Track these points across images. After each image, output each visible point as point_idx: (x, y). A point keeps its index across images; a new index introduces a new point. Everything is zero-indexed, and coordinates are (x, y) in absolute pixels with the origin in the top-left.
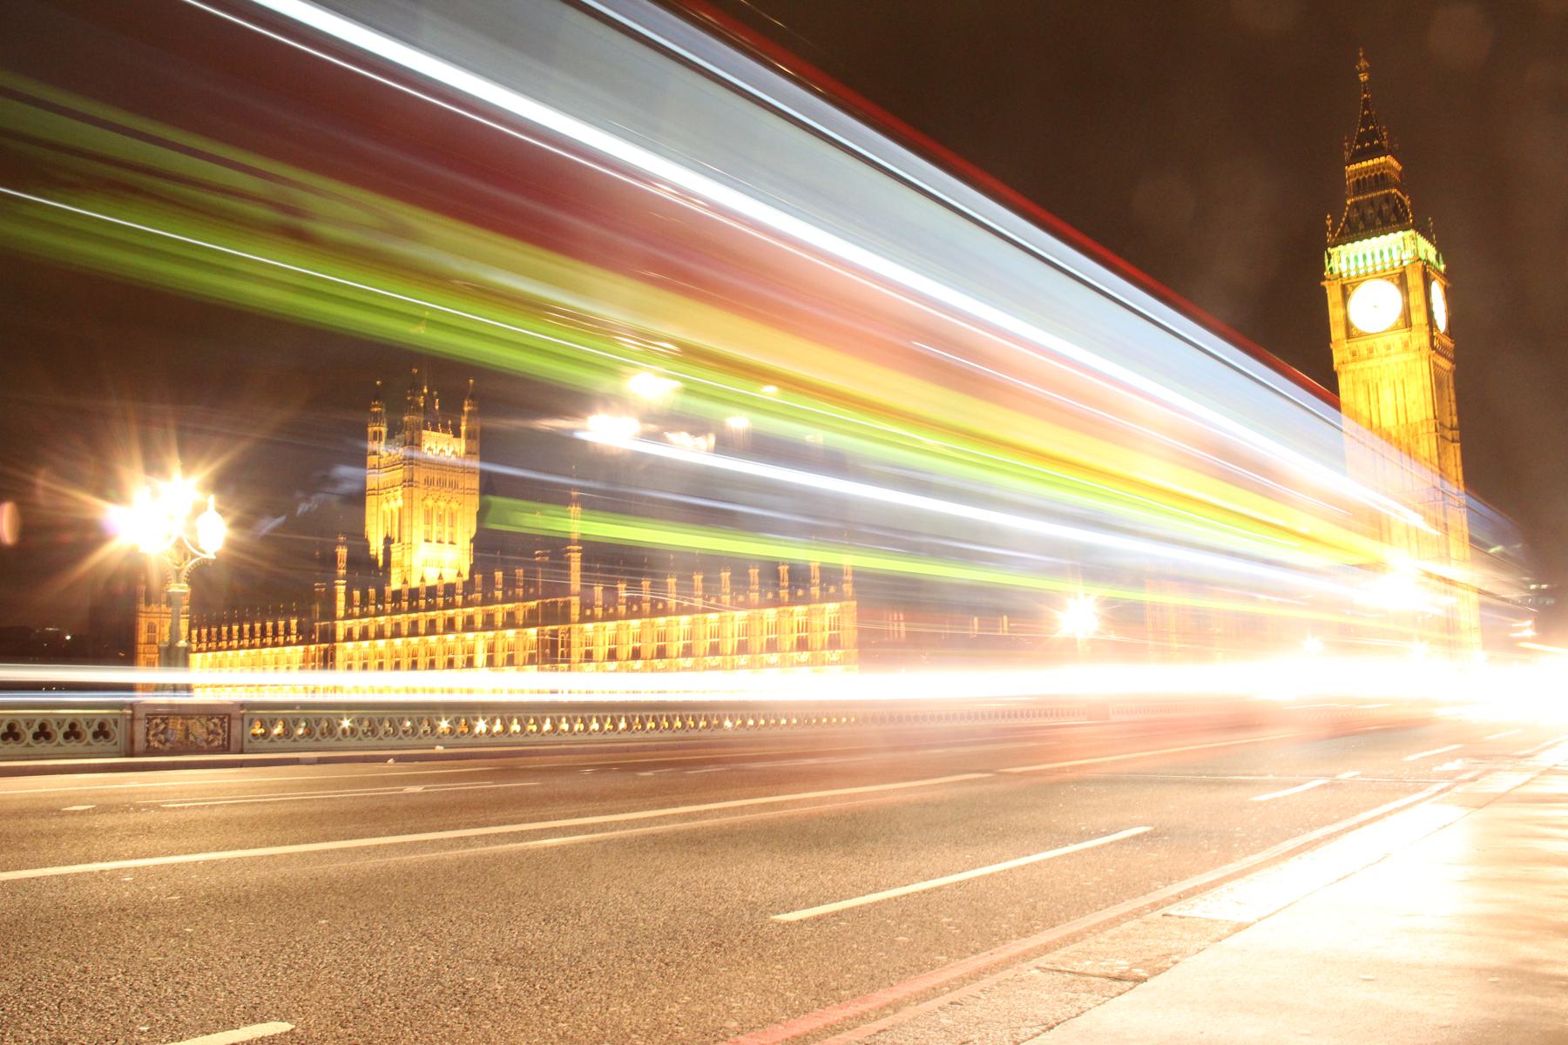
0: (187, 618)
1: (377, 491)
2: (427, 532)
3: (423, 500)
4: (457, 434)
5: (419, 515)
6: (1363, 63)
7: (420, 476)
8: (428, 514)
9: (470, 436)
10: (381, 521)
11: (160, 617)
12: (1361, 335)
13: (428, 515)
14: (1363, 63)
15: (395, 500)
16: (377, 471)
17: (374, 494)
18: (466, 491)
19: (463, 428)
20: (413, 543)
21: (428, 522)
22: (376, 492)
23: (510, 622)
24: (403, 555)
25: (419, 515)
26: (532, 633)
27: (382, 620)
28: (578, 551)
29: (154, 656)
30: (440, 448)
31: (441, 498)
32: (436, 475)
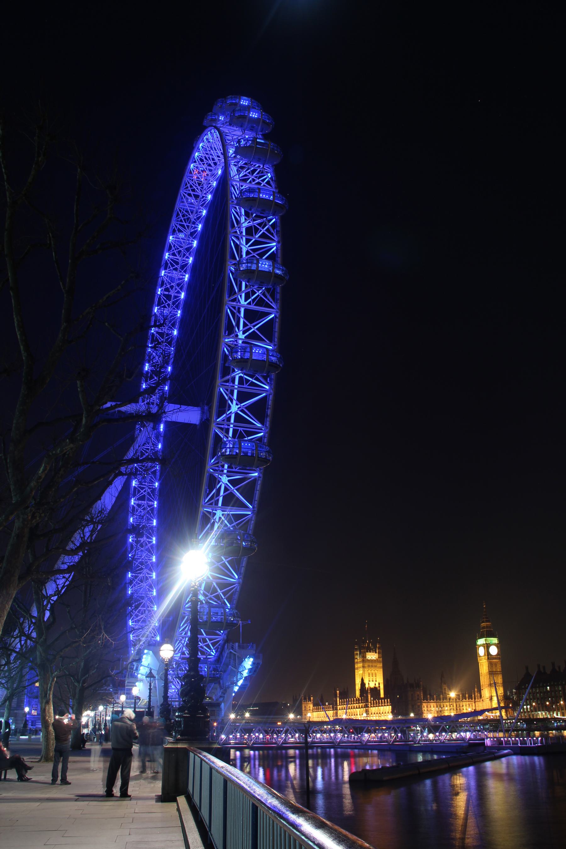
1: (358, 668)
4: (376, 653)
6: (484, 604)
7: (366, 665)
8: (369, 674)
9: (378, 654)
12: (481, 656)
14: (484, 604)
18: (379, 667)
19: (377, 651)
21: (369, 676)
23: (362, 707)
25: (367, 675)
26: (365, 709)
27: (344, 706)
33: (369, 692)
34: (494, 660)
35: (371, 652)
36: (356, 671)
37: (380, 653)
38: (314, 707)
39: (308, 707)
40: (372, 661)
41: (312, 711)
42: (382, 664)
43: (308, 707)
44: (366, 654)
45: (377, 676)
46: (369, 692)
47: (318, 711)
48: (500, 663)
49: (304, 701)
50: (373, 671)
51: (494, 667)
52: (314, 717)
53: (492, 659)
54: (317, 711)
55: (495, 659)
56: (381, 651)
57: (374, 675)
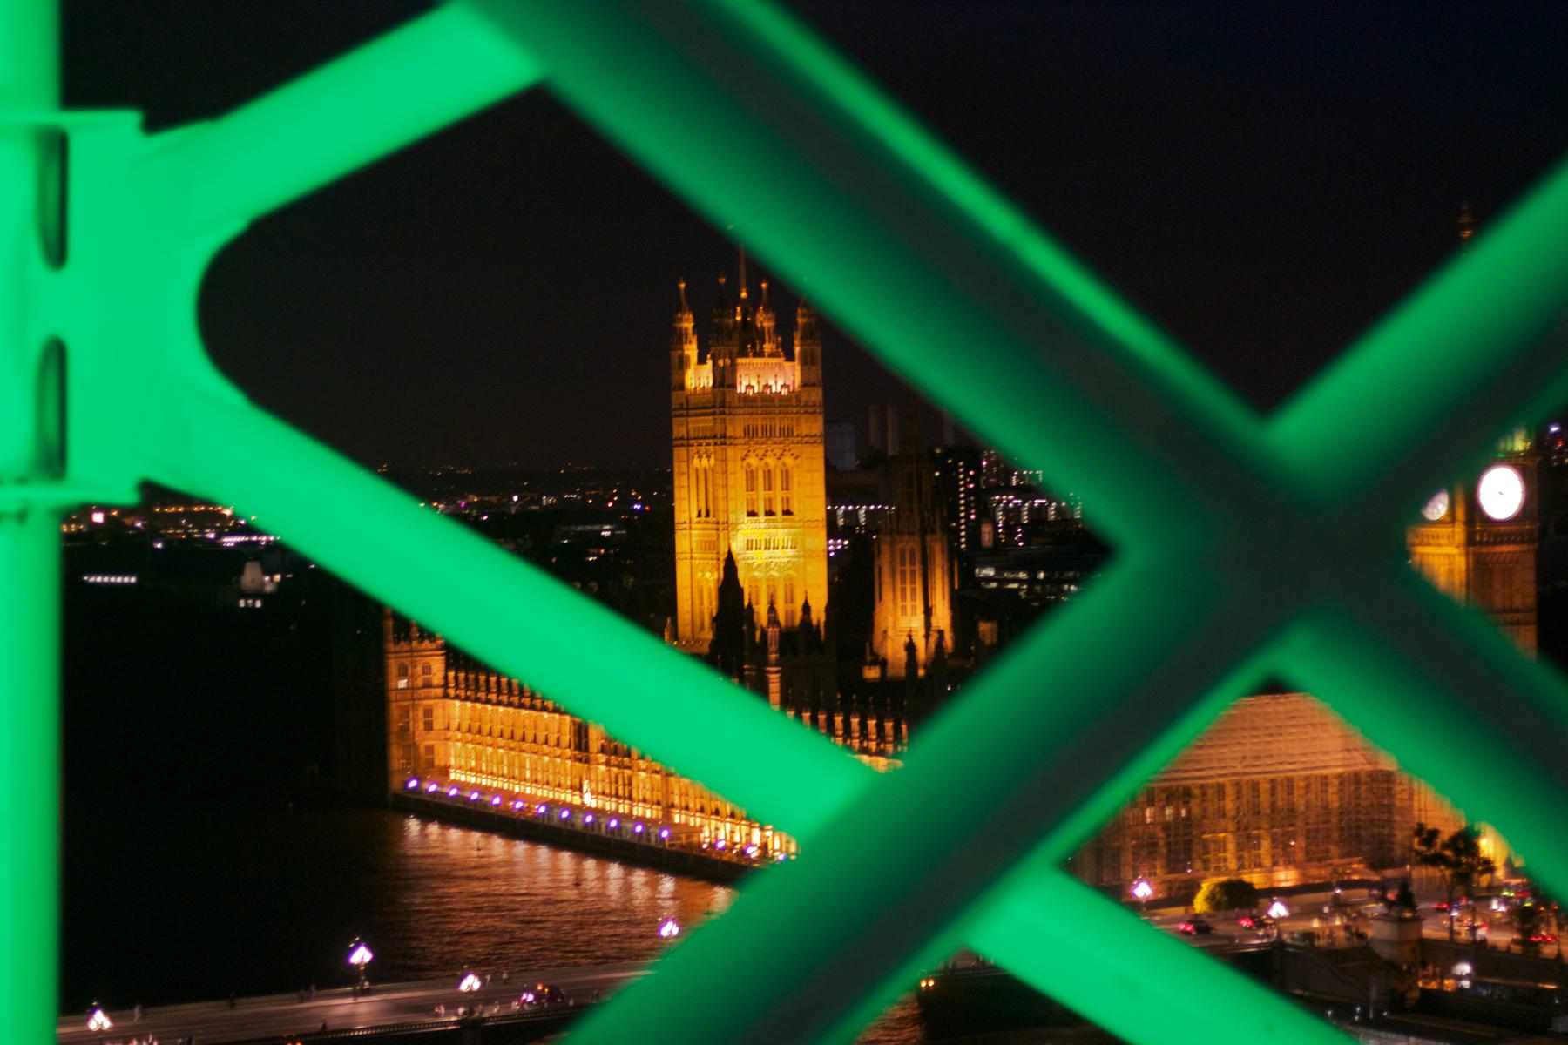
0: (442, 655)
1: (687, 441)
2: (751, 502)
3: (743, 459)
4: (790, 357)
5: (738, 479)
7: (736, 427)
8: (751, 476)
9: (804, 363)
10: (693, 480)
11: (411, 656)
13: (752, 477)
15: (708, 457)
16: (685, 412)
17: (683, 445)
18: (809, 440)
19: (797, 350)
20: (730, 521)
21: (751, 488)
22: (685, 442)
24: (718, 538)
25: (738, 479)
28: (777, 672)
29: (407, 703)
30: (763, 383)
31: (769, 453)
32: (759, 422)
33: (773, 656)
34: (1498, 549)
35: (760, 354)
36: (679, 453)
37: (813, 363)
38: (451, 674)
39: (419, 669)
40: (766, 402)
41: (440, 691)
42: (820, 419)
43: (419, 669)
44: (734, 366)
45: (795, 488)
46: (773, 656)
47: (477, 700)
48: (1530, 561)
49: (397, 641)
50: (771, 461)
51: (1497, 585)
52: (454, 725)
53: (1487, 544)
54: (467, 699)
55: (1508, 543)
56: (818, 350)
57: (778, 481)
